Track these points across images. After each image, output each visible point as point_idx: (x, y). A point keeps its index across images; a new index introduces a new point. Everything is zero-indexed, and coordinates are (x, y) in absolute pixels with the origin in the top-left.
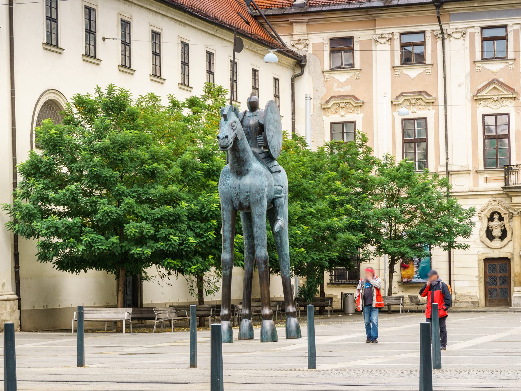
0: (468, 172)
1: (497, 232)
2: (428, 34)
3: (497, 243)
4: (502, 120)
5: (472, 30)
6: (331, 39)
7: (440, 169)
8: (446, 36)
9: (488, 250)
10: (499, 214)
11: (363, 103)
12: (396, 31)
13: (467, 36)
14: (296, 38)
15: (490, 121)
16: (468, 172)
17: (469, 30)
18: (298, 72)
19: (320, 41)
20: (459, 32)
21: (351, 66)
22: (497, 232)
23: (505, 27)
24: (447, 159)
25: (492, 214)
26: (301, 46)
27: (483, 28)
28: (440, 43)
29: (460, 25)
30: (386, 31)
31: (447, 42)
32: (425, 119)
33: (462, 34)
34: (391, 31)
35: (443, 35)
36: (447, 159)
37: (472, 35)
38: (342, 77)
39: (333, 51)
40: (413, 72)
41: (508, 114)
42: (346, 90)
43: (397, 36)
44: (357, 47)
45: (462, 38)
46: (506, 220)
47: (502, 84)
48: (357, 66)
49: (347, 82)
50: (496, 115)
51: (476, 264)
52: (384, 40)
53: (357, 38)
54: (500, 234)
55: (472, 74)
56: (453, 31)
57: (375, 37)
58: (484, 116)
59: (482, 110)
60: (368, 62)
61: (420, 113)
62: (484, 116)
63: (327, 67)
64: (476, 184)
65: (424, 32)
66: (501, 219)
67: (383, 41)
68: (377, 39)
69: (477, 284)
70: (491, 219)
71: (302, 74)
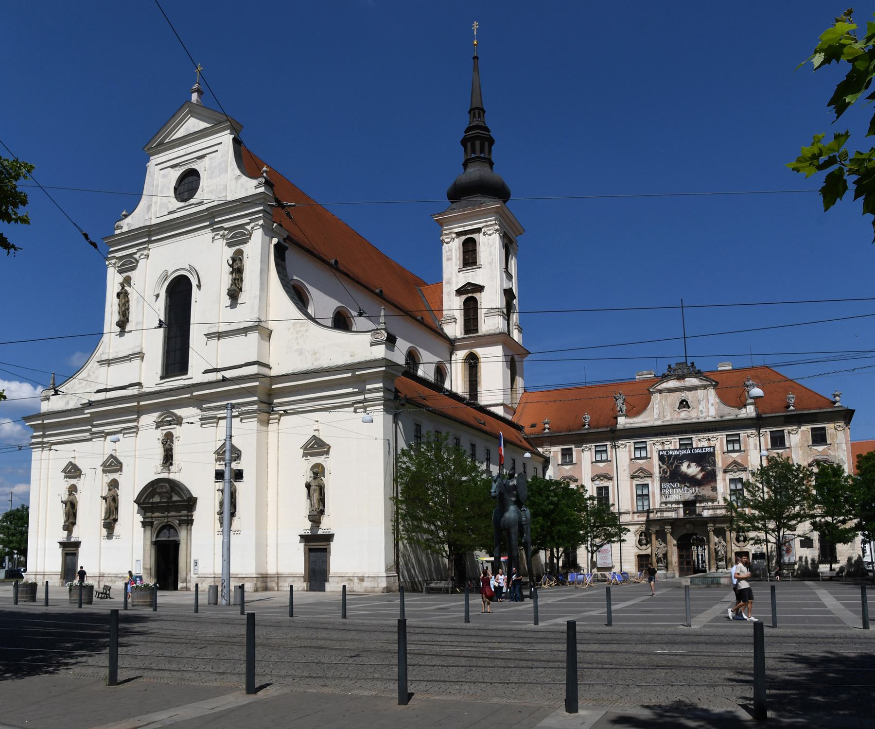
0: (629, 513)
3: (644, 547)
16: (629, 513)
35: (615, 447)
37: (630, 446)
38: (567, 467)
39: (563, 455)
48: (574, 462)
55: (629, 465)
60: (579, 459)
63: (560, 462)
64: (633, 518)
70: (641, 535)
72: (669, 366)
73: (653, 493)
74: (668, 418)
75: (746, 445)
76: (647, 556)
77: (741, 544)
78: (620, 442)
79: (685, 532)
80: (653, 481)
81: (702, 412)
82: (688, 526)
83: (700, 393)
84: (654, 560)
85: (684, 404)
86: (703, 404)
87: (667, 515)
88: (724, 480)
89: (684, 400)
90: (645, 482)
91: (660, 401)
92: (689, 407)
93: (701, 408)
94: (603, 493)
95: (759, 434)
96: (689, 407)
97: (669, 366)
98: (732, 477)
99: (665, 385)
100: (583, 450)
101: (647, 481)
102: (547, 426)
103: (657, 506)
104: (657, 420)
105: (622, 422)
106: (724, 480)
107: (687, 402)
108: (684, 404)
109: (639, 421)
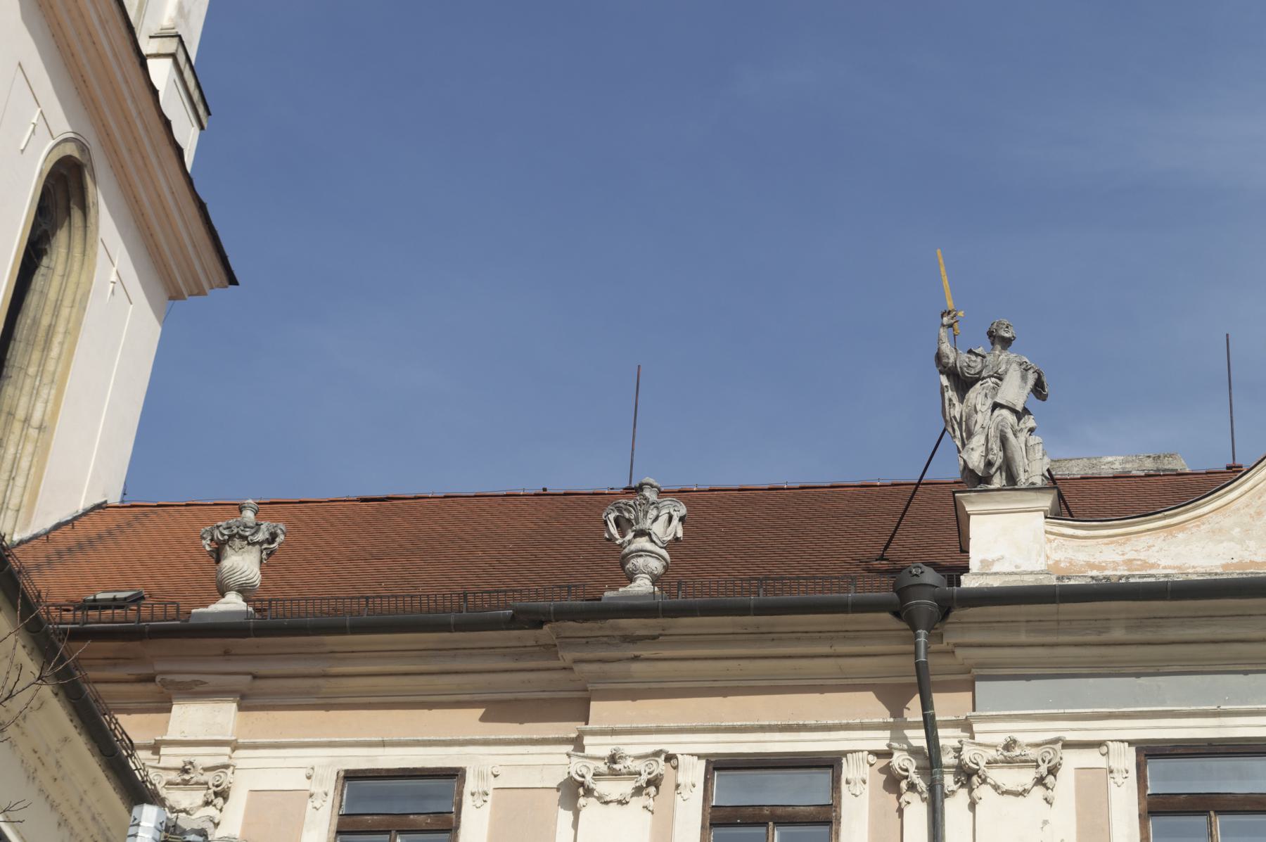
5: (1091, 758)
6: (350, 776)
8: (949, 781)
12: (692, 749)
13: (1065, 783)
17: (1072, 760)
19: (295, 781)
20: (1024, 762)
27: (1149, 752)
28: (917, 812)
29: (1029, 734)
30: (633, 746)
31: (955, 808)
33: (1043, 769)
34: (669, 743)
43: (693, 773)
45: (1039, 792)
52: (624, 788)
53: (481, 776)
56: (992, 754)
57: (577, 767)
68: (589, 779)
78: (992, 734)
100: (573, 792)
105: (1010, 543)
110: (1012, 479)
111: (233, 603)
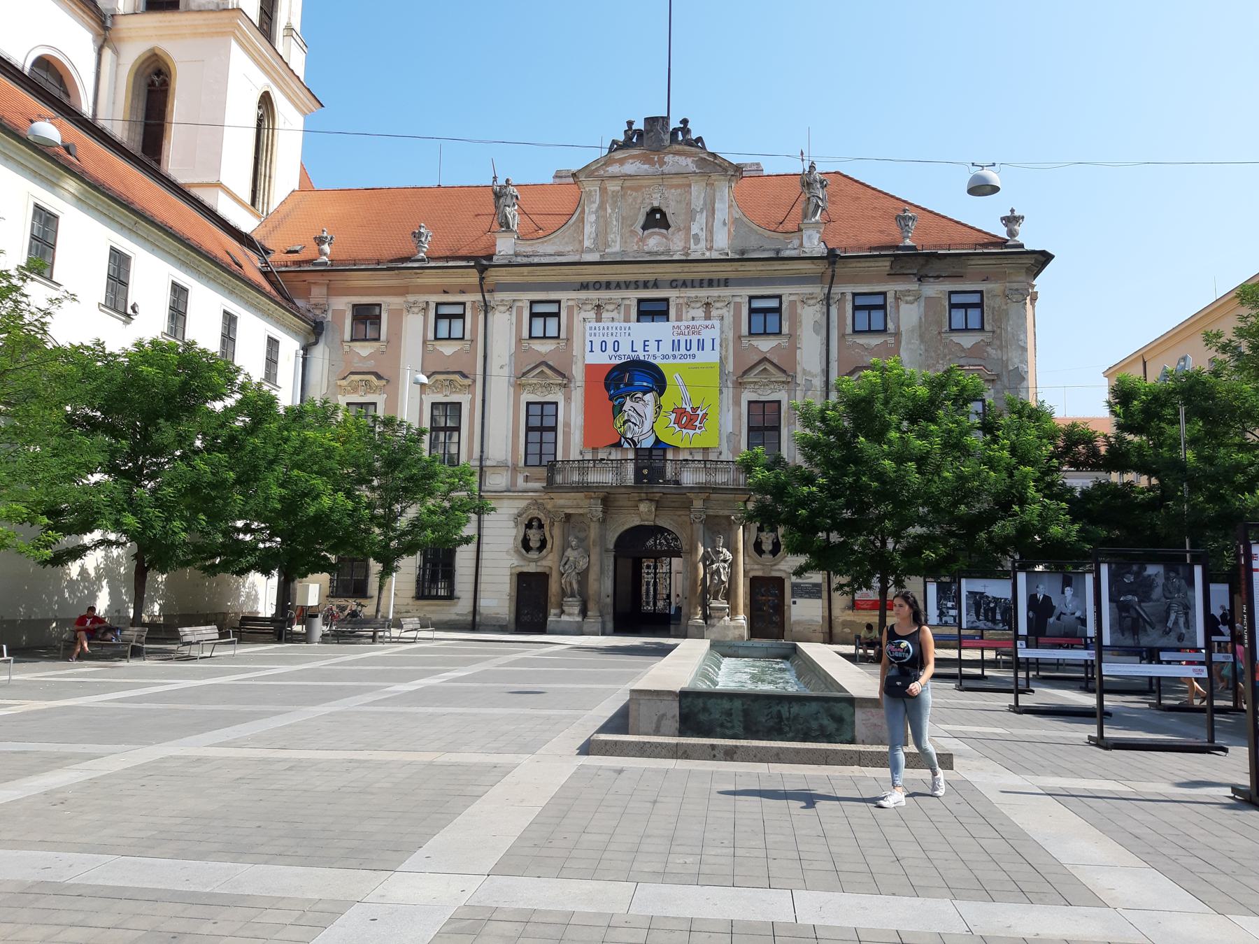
1: (534, 543)
2: (468, 305)
3: (534, 555)
4: (549, 410)
6: (354, 306)
7: (472, 463)
9: (522, 563)
10: (539, 520)
11: (388, 381)
13: (514, 309)
14: (313, 301)
15: (536, 410)
18: (312, 340)
21: (378, 339)
22: (534, 543)
23: (559, 302)
24: (482, 451)
25: (531, 521)
26: (317, 312)
28: (481, 317)
31: (489, 315)
32: (460, 404)
35: (486, 308)
36: (482, 451)
37: (520, 310)
38: (364, 350)
40: (448, 349)
41: (556, 403)
42: (370, 365)
43: (432, 306)
44: (384, 317)
46: (547, 528)
47: (551, 368)
48: (383, 337)
49: (370, 356)
50: (542, 404)
51: (507, 579)
54: (538, 545)
58: (528, 404)
59: (527, 397)
61: (454, 398)
62: (528, 404)
63: (347, 336)
64: (514, 482)
65: (464, 304)
66: (541, 526)
67: (416, 310)
69: (507, 604)
70: (529, 526)
71: (316, 343)
72: (630, 123)
73: (567, 425)
74: (616, 248)
75: (795, 322)
76: (543, 577)
77: (767, 557)
79: (636, 522)
80: (568, 399)
81: (696, 237)
82: (643, 507)
83: (697, 193)
84: (554, 587)
85: (656, 219)
86: (701, 219)
87: (594, 477)
88: (737, 403)
89: (655, 210)
90: (550, 398)
91: (602, 207)
92: (667, 227)
93: (695, 229)
94: (446, 418)
95: (828, 297)
96: (667, 227)
97: (630, 123)
98: (754, 397)
99: (614, 169)
101: (558, 396)
102: (326, 248)
103: (574, 455)
104: (590, 250)
106: (737, 403)
107: (663, 215)
108: (656, 219)
109: (546, 249)
110: (508, 227)
111: (325, 259)
